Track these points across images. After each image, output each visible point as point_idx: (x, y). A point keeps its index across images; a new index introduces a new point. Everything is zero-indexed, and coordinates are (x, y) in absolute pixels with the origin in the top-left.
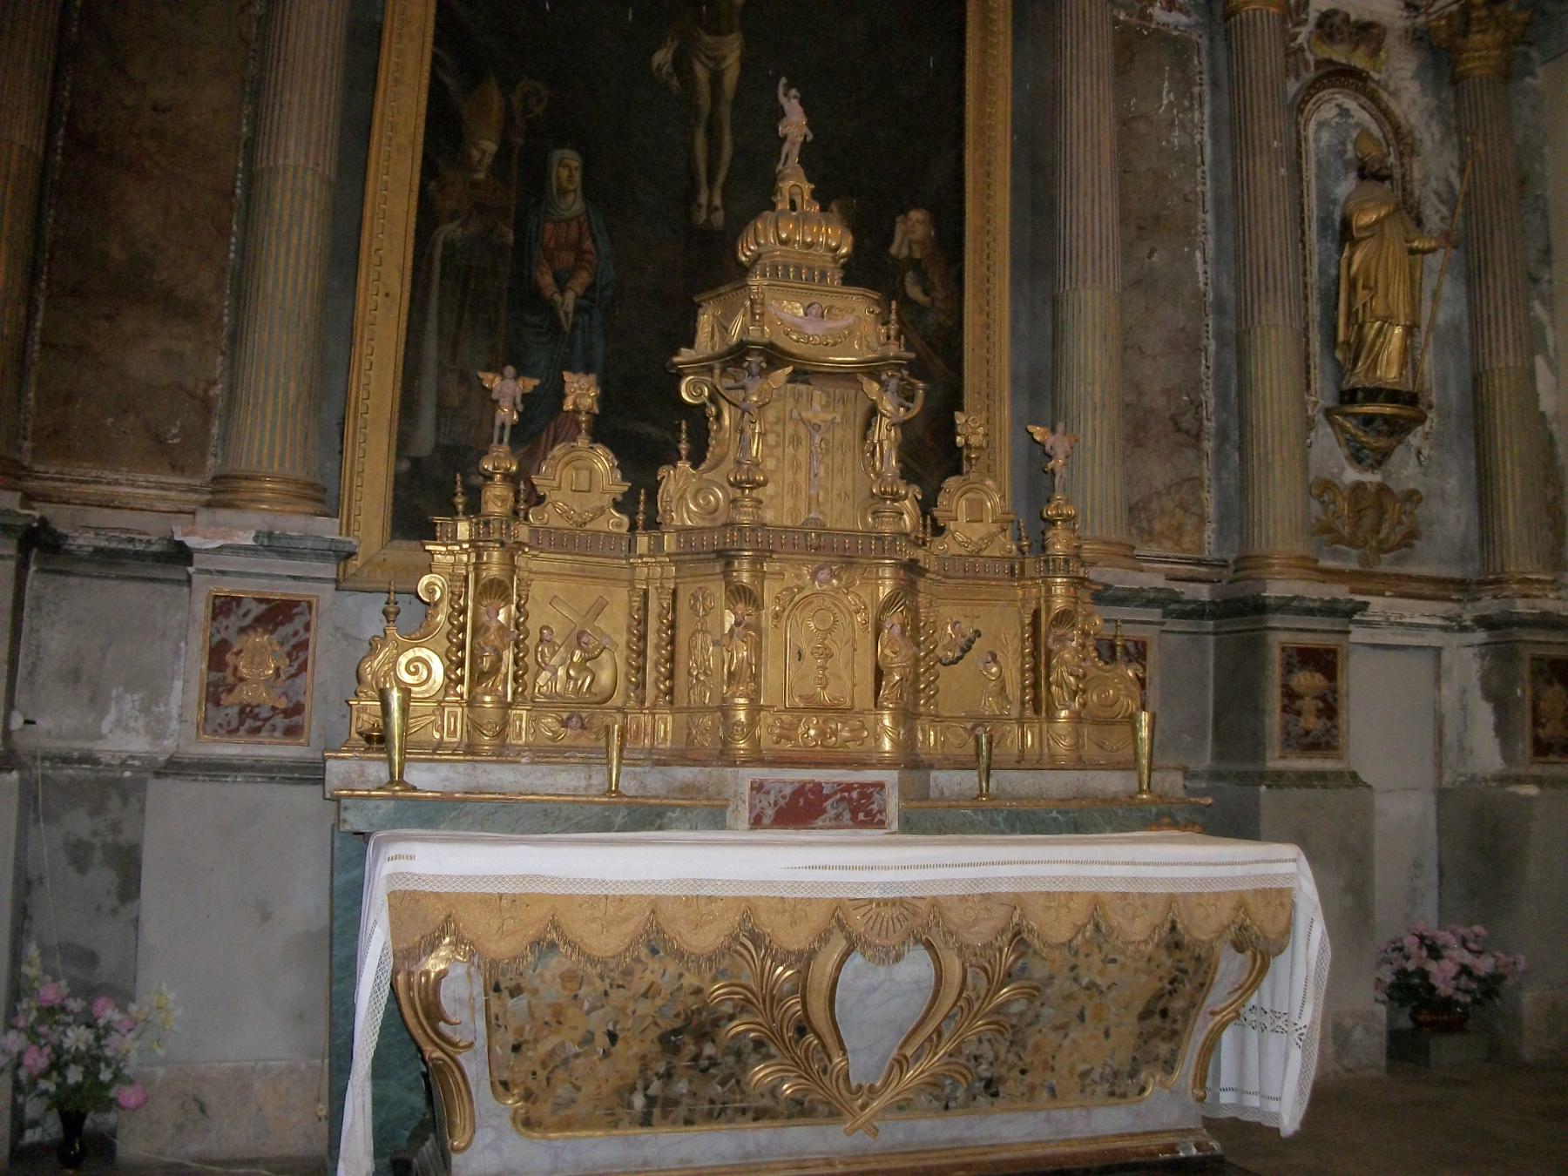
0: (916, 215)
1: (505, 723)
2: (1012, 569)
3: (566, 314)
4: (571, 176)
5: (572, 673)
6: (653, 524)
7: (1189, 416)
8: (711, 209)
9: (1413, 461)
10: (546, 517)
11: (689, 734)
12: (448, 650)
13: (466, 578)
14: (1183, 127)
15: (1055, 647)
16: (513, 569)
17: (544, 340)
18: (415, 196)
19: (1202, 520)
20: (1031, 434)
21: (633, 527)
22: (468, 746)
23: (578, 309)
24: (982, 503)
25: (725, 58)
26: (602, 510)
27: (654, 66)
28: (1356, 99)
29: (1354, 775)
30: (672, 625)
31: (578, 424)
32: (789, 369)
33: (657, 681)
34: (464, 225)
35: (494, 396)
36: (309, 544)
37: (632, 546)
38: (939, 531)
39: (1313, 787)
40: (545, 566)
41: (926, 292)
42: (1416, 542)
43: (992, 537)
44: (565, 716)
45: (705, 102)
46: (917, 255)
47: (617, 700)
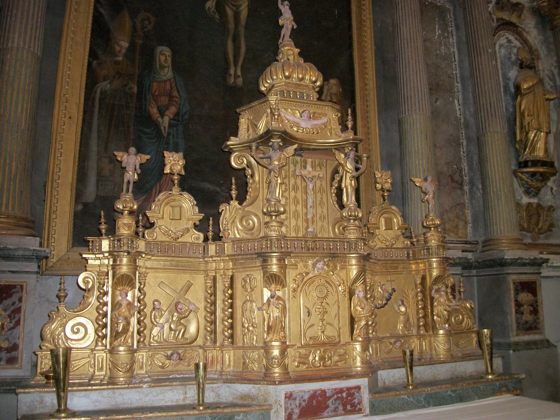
1: (133, 362)
3: (165, 127)
4: (166, 59)
5: (172, 326)
6: (217, 238)
7: (457, 174)
8: (236, 77)
9: (549, 192)
10: (157, 235)
11: (244, 363)
12: (97, 319)
13: (107, 274)
14: (445, 45)
15: (436, 296)
16: (134, 267)
17: (155, 140)
18: (85, 67)
19: (466, 223)
21: (206, 239)
22: (110, 378)
23: (170, 126)
25: (240, 6)
26: (188, 230)
27: (207, 8)
28: (513, 35)
29: (548, 341)
30: (232, 297)
31: (173, 181)
32: (295, 146)
33: (223, 331)
34: (111, 83)
35: (123, 165)
36: (21, 253)
37: (205, 250)
39: (532, 349)
40: (155, 264)
42: (553, 229)
43: (397, 238)
44: (169, 353)
45: (232, 26)
47: (200, 341)
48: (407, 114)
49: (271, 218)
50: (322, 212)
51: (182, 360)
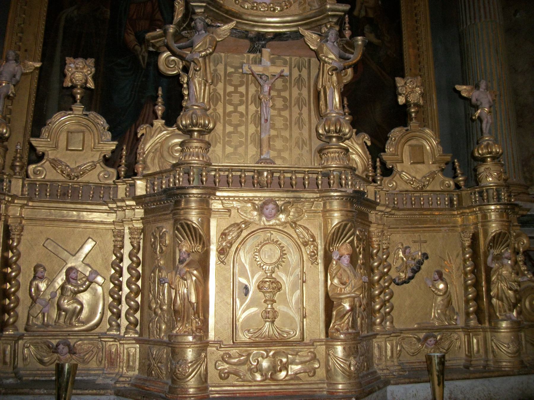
2: (451, 201)
3: (143, 57)
15: (495, 266)
20: (459, 92)
24: (422, 147)
32: (232, 25)
38: (387, 172)
43: (432, 175)
46: (371, 15)
48: (469, 24)
49: (191, 136)
50: (301, 134)
51: (75, 353)
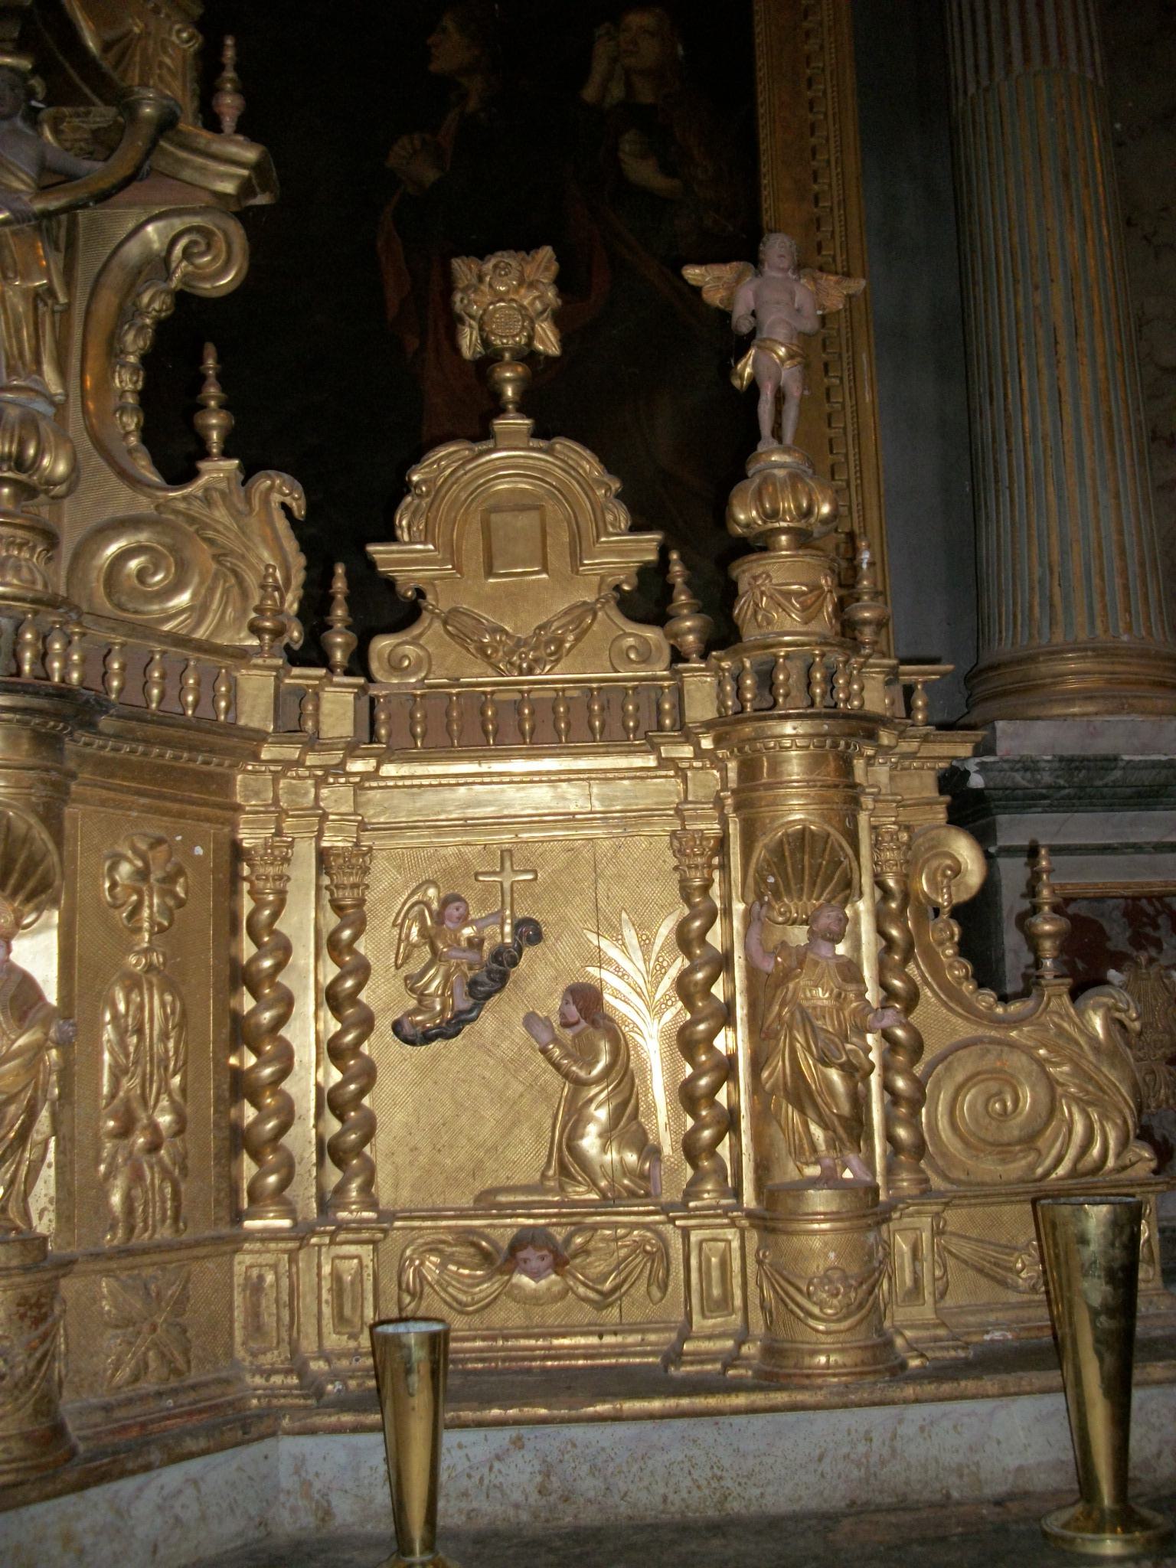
0: (636, 20)
38: (390, 609)
41: (667, 169)
46: (646, 95)
48: (972, 90)
